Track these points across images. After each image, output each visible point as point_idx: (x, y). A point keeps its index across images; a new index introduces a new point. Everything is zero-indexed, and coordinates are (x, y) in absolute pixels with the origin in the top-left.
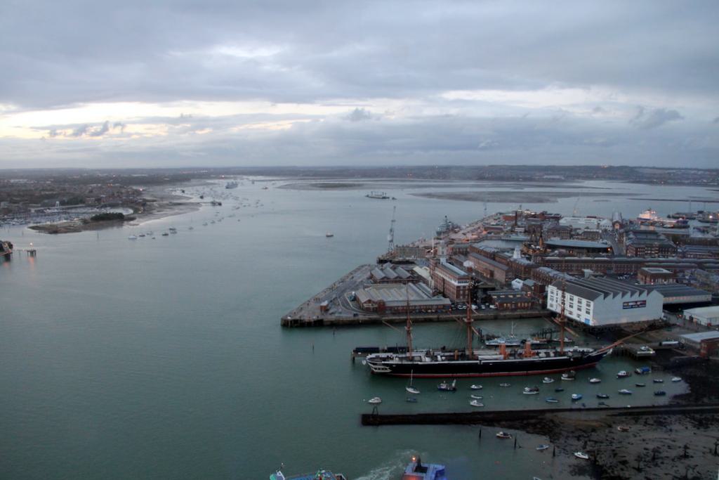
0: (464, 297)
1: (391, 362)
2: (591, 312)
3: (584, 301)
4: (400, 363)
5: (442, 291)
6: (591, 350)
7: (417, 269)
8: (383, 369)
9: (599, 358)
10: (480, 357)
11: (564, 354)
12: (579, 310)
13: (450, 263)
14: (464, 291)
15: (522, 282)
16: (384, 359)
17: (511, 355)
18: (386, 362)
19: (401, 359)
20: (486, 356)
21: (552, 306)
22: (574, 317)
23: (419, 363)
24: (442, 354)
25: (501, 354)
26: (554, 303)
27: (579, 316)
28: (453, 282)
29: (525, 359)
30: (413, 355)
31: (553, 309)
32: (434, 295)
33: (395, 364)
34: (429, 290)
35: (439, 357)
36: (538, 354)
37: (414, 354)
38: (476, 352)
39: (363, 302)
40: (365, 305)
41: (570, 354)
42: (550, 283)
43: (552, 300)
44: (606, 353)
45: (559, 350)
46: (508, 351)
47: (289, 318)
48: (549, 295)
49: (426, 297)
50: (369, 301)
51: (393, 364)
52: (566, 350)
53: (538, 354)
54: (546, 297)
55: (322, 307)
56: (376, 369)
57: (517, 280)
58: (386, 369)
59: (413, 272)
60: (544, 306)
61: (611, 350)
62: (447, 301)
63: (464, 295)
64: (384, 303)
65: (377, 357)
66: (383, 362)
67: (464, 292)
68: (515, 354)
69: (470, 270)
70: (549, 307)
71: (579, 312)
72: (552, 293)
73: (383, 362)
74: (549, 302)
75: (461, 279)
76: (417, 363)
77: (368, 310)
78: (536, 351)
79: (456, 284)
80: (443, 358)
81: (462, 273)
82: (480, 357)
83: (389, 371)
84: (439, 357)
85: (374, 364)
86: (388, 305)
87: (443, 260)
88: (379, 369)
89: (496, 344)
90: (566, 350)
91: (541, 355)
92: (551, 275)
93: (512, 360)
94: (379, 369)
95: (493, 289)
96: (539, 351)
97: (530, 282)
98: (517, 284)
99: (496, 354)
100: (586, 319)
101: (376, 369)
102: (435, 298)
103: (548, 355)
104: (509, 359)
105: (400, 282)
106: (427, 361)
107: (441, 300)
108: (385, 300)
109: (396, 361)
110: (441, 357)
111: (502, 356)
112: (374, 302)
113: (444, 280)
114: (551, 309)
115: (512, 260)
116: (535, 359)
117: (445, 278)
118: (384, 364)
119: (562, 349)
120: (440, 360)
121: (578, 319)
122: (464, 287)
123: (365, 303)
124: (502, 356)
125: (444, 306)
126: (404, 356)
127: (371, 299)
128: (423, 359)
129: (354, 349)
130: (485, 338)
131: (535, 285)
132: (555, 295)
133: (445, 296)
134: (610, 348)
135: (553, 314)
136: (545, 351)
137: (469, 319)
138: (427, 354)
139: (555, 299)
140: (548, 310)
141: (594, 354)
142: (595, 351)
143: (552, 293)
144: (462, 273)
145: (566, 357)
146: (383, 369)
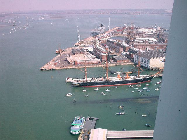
9: (151, 78)
12: (145, 62)
15: (125, 53)
20: (113, 79)
21: (135, 61)
22: (143, 65)
23: (89, 82)
29: (126, 80)
35: (97, 80)
43: (136, 59)
49: (92, 59)
52: (140, 76)
57: (124, 52)
59: (87, 50)
61: (155, 76)
67: (105, 57)
74: (135, 60)
78: (130, 76)
79: (103, 54)
83: (79, 85)
85: (74, 83)
86: (78, 62)
92: (135, 50)
93: (122, 80)
95: (115, 55)
97: (128, 53)
98: (124, 53)
102: (95, 59)
106: (92, 81)
111: (118, 79)
115: (122, 45)
116: (130, 79)
120: (97, 81)
125: (98, 62)
127: (73, 60)
128: (91, 81)
135: (136, 64)
136: (133, 76)
140: (134, 63)
144: (104, 50)
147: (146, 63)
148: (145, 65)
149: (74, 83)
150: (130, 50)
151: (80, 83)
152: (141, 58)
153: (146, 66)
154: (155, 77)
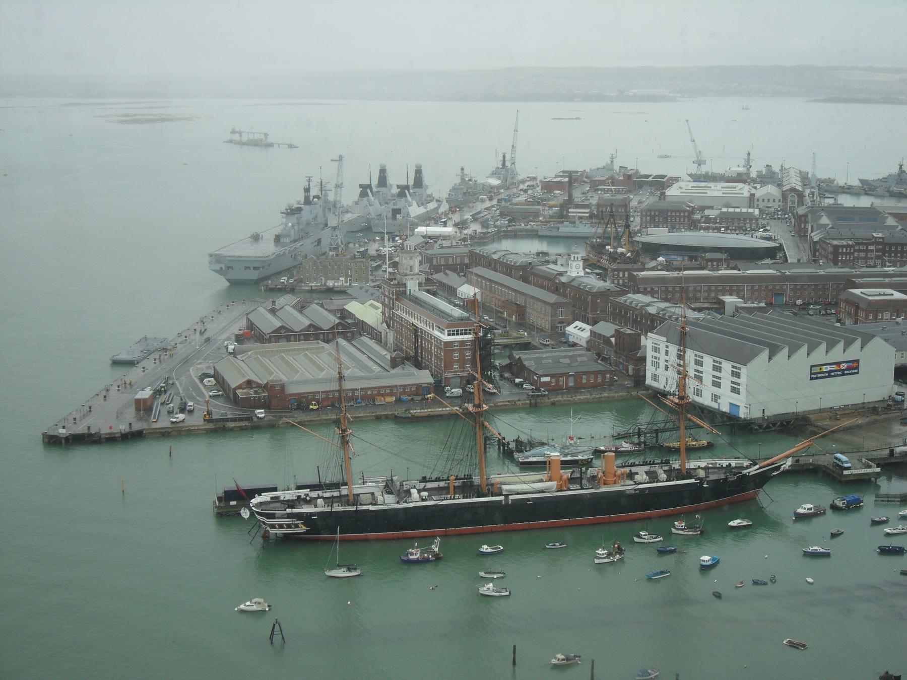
0: (463, 367)
1: (306, 509)
2: (742, 389)
3: (727, 366)
4: (328, 509)
5: (412, 353)
6: (746, 463)
7: (353, 307)
8: (289, 526)
9: (762, 479)
10: (504, 487)
11: (689, 474)
12: (717, 384)
13: (428, 291)
14: (462, 351)
15: (588, 328)
16: (291, 504)
17: (572, 480)
18: (295, 511)
19: (330, 501)
21: (655, 377)
22: (705, 400)
23: (372, 508)
24: (422, 485)
25: (550, 480)
26: (661, 371)
27: (717, 368)
28: (436, 333)
29: (604, 489)
30: (356, 492)
31: (660, 385)
32: (394, 363)
33: (319, 514)
34: (384, 352)
36: (631, 476)
37: (357, 489)
38: (495, 478)
39: (233, 386)
41: (702, 474)
42: (651, 329)
43: (656, 365)
44: (779, 467)
45: (676, 465)
46: (566, 474)
48: (650, 354)
49: (376, 368)
50: (249, 383)
51: (312, 514)
53: (631, 476)
54: (643, 359)
55: (138, 402)
56: (273, 526)
57: (577, 323)
58: (297, 526)
59: (344, 314)
60: (639, 379)
61: (789, 462)
62: (425, 377)
63: (462, 362)
64: (283, 386)
65: (275, 499)
66: (289, 511)
68: (581, 478)
69: (470, 305)
70: (649, 381)
71: (716, 390)
72: (656, 350)
73: (289, 511)
74: (650, 370)
75: (454, 325)
76: (365, 507)
78: (627, 470)
79: (445, 338)
80: (425, 494)
81: (457, 312)
82: (504, 487)
83: (303, 529)
84: (414, 491)
85: (272, 516)
87: (412, 285)
88: (281, 526)
89: (541, 459)
90: (692, 465)
91: (638, 478)
92: (652, 310)
94: (281, 526)
96: (634, 469)
97: (607, 329)
98: (579, 332)
99: (541, 481)
100: (731, 404)
101: (273, 526)
102: (398, 370)
103: (653, 476)
104: (569, 489)
105: (316, 337)
106: (389, 502)
107: (410, 375)
108: (284, 378)
109: (322, 507)
110: (419, 491)
111: (553, 484)
112: (259, 386)
113: (416, 330)
114: (655, 384)
115: (564, 279)
116: (627, 486)
117: (421, 325)
119: (682, 465)
120: (416, 500)
121: (714, 405)
122: (462, 343)
123: (239, 387)
124: (553, 484)
125: (418, 386)
126: (336, 494)
129: (221, 493)
130: (512, 446)
131: (618, 334)
132: (662, 356)
133: (419, 365)
134: (787, 457)
135: (658, 396)
136: (647, 468)
137: (479, 406)
138: (387, 486)
139: (662, 364)
140: (649, 388)
141: (753, 470)
142: (755, 464)
143: (656, 350)
144: (457, 312)
145: (692, 481)
146: (289, 526)
147: (726, 383)
148: (715, 398)
150: (622, 314)
151: (306, 518)
152: (690, 355)
153: (725, 408)
154: (783, 472)
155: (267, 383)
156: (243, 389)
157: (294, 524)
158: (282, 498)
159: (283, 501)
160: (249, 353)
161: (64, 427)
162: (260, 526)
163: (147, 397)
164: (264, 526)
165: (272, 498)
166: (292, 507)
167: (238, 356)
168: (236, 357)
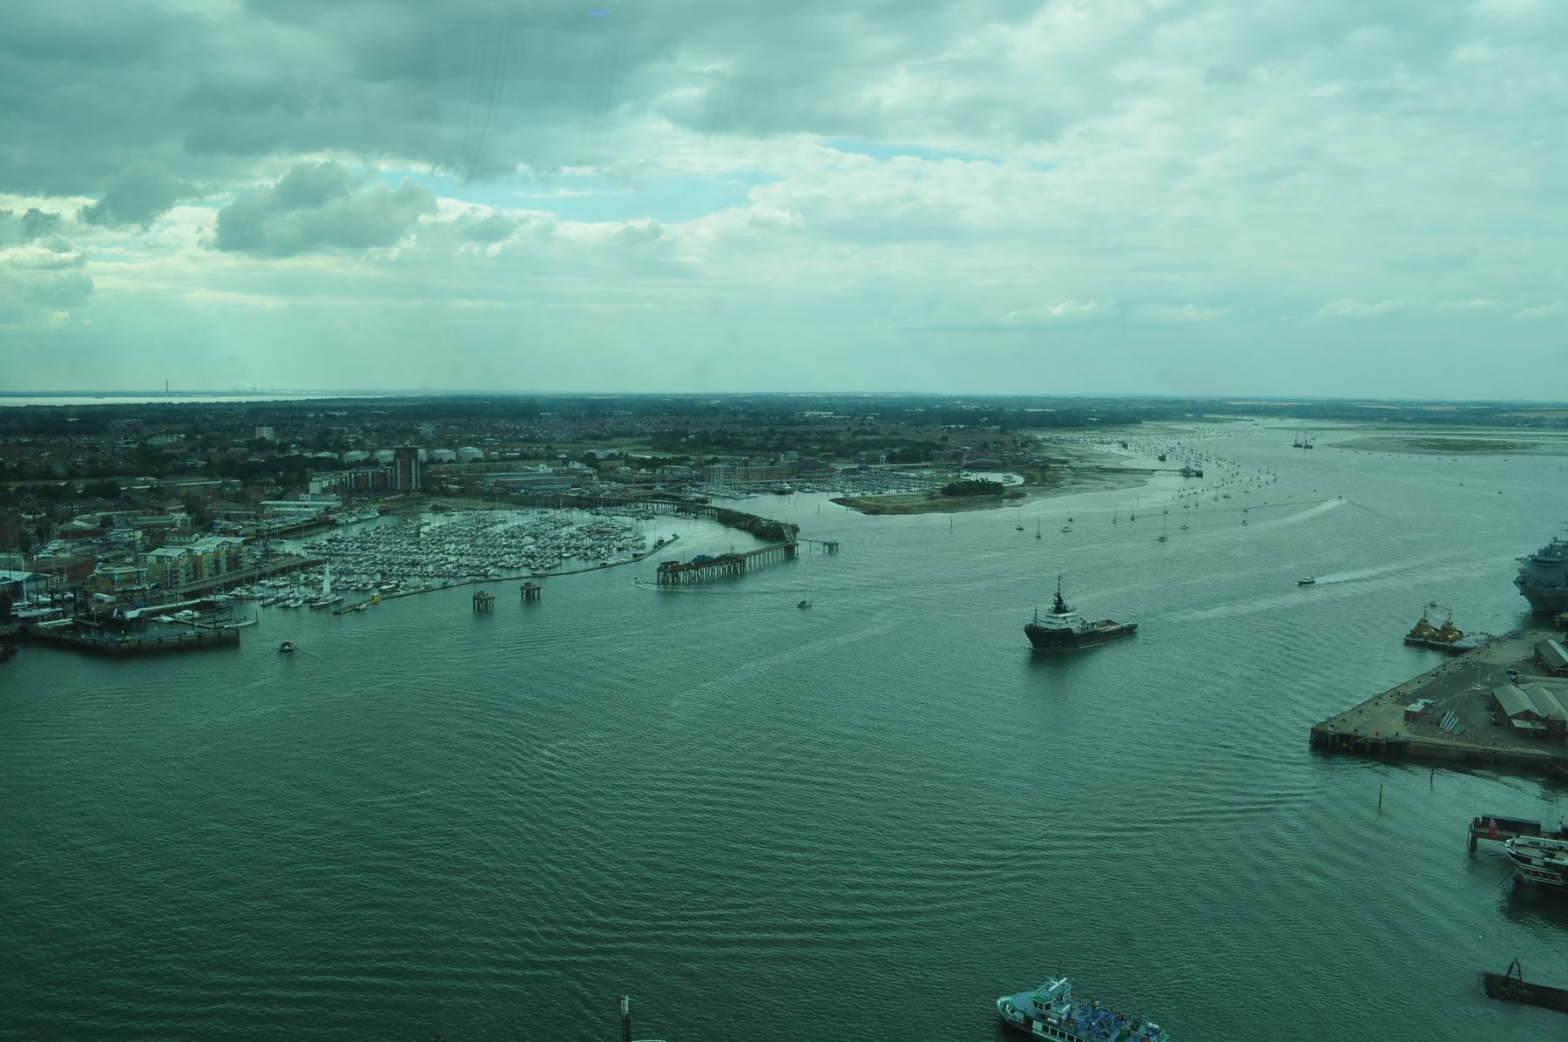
8: (1545, 875)
16: (1551, 853)
39: (1510, 715)
40: (1517, 723)
47: (1332, 729)
50: (1527, 715)
55: (1407, 713)
58: (1553, 877)
66: (1547, 859)
73: (1547, 859)
77: (1522, 733)
83: (1560, 882)
94: (1536, 874)
101: (1527, 872)
112: (1538, 718)
118: (1547, 865)
123: (1516, 717)
149: (1527, 861)
155: (1547, 717)
156: (1520, 719)
157: (1551, 875)
158: (1542, 845)
159: (1542, 848)
160: (1532, 684)
161: (1332, 726)
162: (1514, 868)
163: (1418, 710)
164: (1517, 869)
165: (1530, 843)
166: (1552, 856)
167: (1520, 686)
168: (1518, 687)
